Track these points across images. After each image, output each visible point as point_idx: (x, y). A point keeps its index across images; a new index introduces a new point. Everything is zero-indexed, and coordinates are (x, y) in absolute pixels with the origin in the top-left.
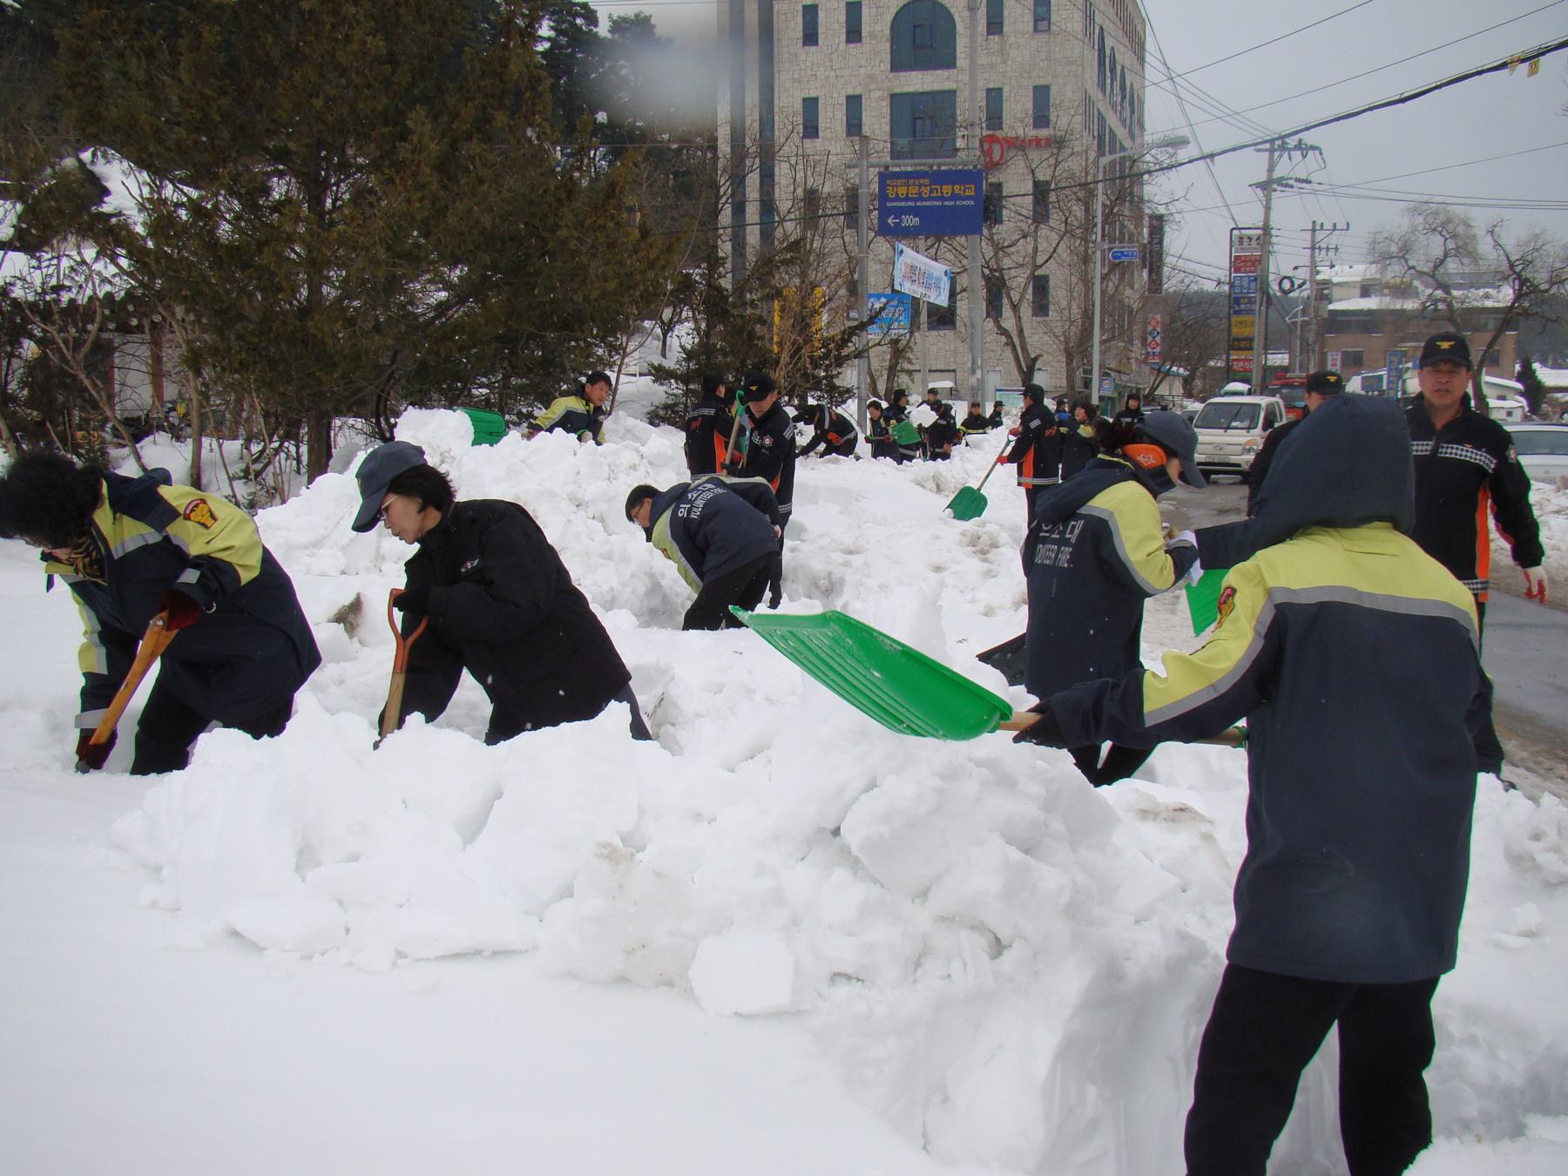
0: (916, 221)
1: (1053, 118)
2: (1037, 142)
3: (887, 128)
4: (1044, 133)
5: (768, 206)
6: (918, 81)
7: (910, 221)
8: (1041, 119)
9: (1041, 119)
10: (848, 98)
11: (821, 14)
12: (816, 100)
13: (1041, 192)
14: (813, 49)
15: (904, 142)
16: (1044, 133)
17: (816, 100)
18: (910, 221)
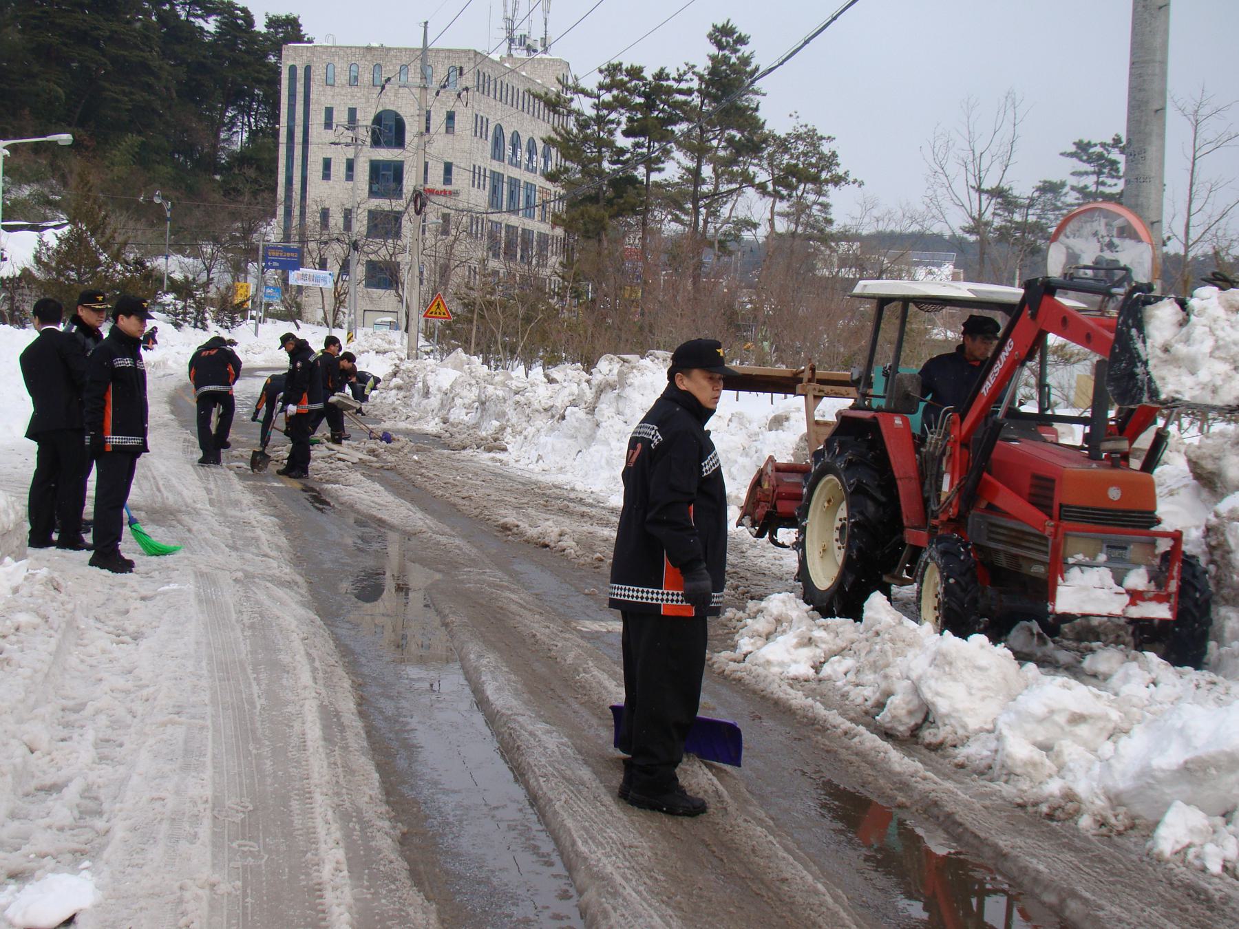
0: (277, 264)
1: (453, 181)
2: (444, 193)
3: (367, 178)
4: (448, 188)
6: (386, 154)
7: (276, 264)
8: (448, 179)
9: (448, 179)
10: (348, 160)
11: (335, 113)
12: (330, 159)
13: (446, 218)
14: (330, 131)
15: (375, 188)
17: (330, 159)
18: (276, 264)
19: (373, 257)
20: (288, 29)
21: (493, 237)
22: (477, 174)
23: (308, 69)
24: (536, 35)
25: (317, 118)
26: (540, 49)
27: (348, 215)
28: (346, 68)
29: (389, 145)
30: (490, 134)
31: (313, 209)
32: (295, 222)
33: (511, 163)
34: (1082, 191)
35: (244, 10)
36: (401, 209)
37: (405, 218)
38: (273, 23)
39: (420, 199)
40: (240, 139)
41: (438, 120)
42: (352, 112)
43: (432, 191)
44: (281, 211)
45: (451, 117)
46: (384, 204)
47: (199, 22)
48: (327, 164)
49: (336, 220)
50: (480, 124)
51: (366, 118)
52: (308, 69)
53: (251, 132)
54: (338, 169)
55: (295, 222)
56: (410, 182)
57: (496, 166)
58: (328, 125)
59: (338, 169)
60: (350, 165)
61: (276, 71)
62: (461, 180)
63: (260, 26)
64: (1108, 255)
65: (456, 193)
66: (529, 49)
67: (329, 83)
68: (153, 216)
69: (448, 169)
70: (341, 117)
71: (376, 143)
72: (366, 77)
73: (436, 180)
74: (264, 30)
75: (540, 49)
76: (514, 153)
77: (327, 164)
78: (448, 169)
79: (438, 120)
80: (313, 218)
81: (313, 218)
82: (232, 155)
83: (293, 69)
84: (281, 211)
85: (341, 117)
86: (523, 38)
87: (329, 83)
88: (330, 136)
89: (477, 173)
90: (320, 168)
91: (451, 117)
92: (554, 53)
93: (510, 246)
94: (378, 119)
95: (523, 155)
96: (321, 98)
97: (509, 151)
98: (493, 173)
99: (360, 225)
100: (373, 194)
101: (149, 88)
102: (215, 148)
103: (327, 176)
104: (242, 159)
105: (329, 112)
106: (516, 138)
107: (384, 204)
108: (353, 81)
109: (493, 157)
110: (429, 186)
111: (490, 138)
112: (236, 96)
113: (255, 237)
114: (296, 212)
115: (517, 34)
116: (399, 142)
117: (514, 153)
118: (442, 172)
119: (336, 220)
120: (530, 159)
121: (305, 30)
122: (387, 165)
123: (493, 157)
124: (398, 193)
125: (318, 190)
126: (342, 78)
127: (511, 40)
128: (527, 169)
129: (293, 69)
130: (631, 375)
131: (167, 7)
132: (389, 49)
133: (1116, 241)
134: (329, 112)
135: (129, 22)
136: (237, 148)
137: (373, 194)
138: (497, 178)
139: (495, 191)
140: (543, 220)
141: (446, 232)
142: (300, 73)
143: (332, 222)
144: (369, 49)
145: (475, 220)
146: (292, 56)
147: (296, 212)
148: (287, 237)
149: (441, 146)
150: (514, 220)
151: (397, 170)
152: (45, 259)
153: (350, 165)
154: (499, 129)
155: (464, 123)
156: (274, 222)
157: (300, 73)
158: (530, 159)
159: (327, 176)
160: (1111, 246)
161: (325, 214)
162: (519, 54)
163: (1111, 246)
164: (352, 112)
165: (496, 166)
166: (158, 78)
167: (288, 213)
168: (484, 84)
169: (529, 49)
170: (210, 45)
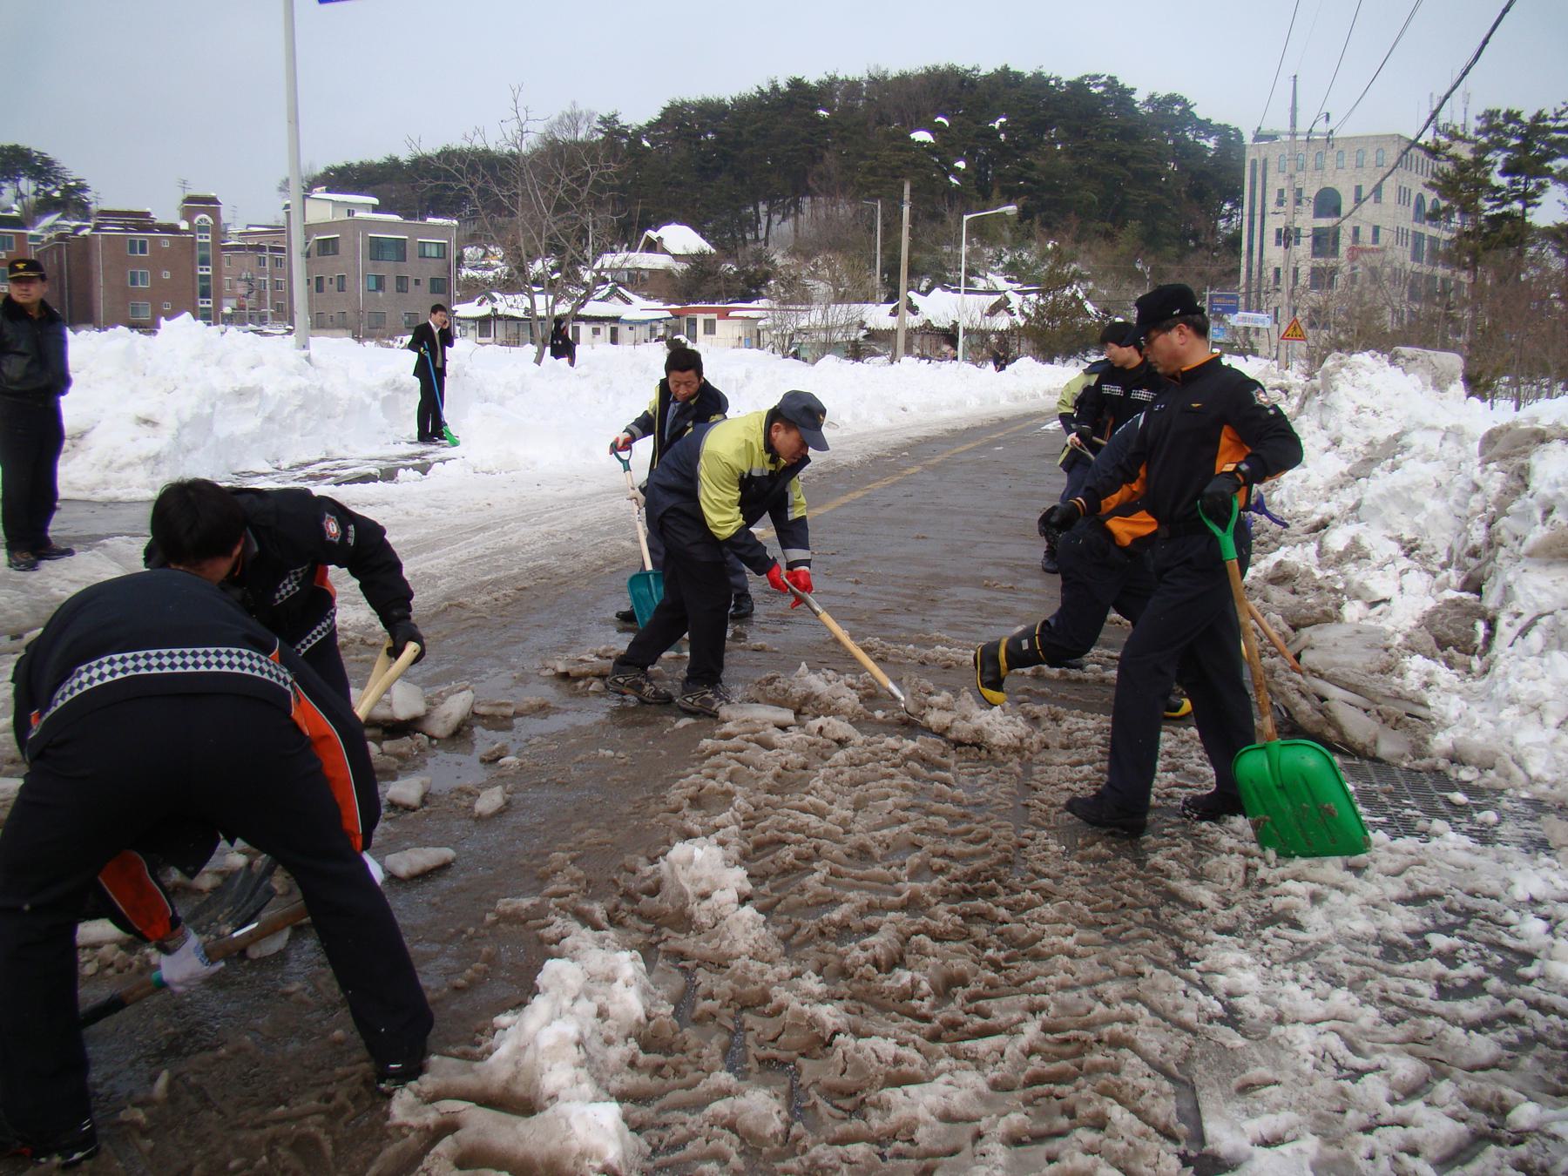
4: (1376, 246)
6: (1324, 223)
15: (1317, 248)
16: (1376, 246)
22: (1400, 233)
35: (1236, 130)
46: (1321, 262)
47: (1203, 142)
51: (1311, 192)
52: (1265, 161)
56: (1345, 242)
65: (1383, 250)
69: (1376, 230)
71: (1318, 214)
78: (1376, 230)
83: (1254, 162)
98: (1414, 232)
99: (1304, 279)
100: (1314, 254)
107: (1321, 262)
110: (1360, 245)
111: (1412, 205)
116: (1336, 211)
118: (1371, 234)
129: (1254, 162)
130: (1338, 376)
151: (1335, 233)
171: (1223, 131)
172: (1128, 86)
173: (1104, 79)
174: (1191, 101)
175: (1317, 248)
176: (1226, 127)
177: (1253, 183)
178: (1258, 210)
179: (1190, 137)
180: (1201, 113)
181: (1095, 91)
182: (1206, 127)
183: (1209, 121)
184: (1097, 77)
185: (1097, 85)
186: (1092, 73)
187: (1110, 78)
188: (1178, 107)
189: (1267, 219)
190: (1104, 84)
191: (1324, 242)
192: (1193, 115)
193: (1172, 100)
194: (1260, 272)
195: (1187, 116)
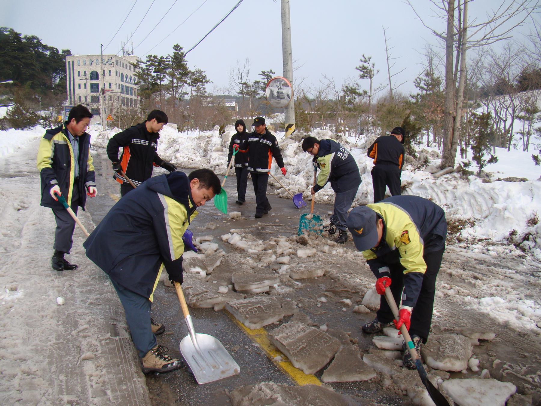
4: (111, 89)
5: (74, 98)
6: (94, 82)
8: (110, 87)
9: (110, 87)
13: (111, 96)
15: (92, 90)
19: (93, 107)
20: (68, 52)
21: (123, 101)
22: (117, 85)
23: (73, 62)
24: (130, 50)
25: (76, 74)
26: (131, 53)
27: (86, 97)
28: (83, 61)
29: (95, 79)
30: (120, 75)
31: (76, 96)
32: (73, 100)
33: (126, 82)
34: (264, 83)
35: (56, 49)
36: (98, 95)
37: (100, 97)
38: (64, 51)
39: (104, 91)
40: (57, 81)
41: (107, 73)
42: (85, 72)
43: (106, 90)
44: (69, 97)
45: (110, 71)
46: (95, 94)
47: (45, 52)
48: (80, 85)
49: (83, 99)
50: (117, 73)
51: (88, 73)
52: (73, 62)
53: (60, 79)
54: (83, 86)
55: (73, 100)
56: (100, 88)
57: (122, 83)
58: (79, 75)
59: (83, 86)
60: (85, 85)
61: (65, 63)
62: (114, 87)
63: (61, 52)
64: (280, 91)
65: (113, 90)
66: (129, 54)
67: (79, 65)
68: (36, 101)
69: (110, 84)
70: (82, 73)
71: (92, 79)
72: (88, 63)
73: (107, 87)
74: (62, 53)
75: (131, 53)
76: (127, 80)
77: (80, 85)
78: (110, 84)
79: (107, 73)
80: (77, 99)
81: (77, 99)
82: (56, 85)
83: (69, 62)
84: (69, 97)
85: (82, 73)
86: (127, 52)
87: (79, 65)
88: (80, 78)
89: (117, 85)
90: (78, 86)
91: (110, 71)
92: (135, 55)
93: (127, 102)
94: (92, 73)
95: (129, 80)
96: (77, 69)
97: (125, 79)
99: (89, 100)
100: (92, 92)
101: (33, 69)
102: (51, 83)
103: (80, 88)
104: (58, 85)
105: (79, 72)
106: (127, 76)
107: (95, 94)
108: (85, 64)
109: (121, 81)
112: (55, 70)
113: (63, 105)
114: (73, 97)
115: (125, 51)
116: (97, 78)
117: (127, 80)
119: (83, 99)
120: (131, 81)
121: (72, 53)
122: (95, 84)
123: (121, 81)
124: (98, 91)
125: (77, 91)
126: (82, 63)
127: (124, 52)
128: (130, 83)
129: (69, 62)
131: (37, 49)
132: (93, 56)
133: (282, 87)
134: (79, 72)
135: (27, 53)
136: (57, 83)
137: (92, 92)
138: (122, 86)
139: (122, 89)
140: (135, 96)
141: (111, 100)
142: (71, 63)
143: (82, 99)
144: (88, 56)
145: (118, 97)
146: (69, 59)
147: (73, 97)
148: (71, 104)
149: (107, 79)
150: (127, 96)
151: (97, 85)
152: (9, 113)
153: (85, 85)
154: (122, 74)
155: (113, 74)
156: (67, 101)
157: (71, 63)
158: (131, 81)
159: (80, 88)
160: (281, 88)
161: (80, 98)
162: (126, 55)
163: (281, 88)
164: (85, 72)
165: (122, 83)
166: (36, 67)
167: (71, 98)
168: (118, 63)
169: (129, 54)
170: (48, 58)
171: (52, 49)
172: (18, 33)
173: (9, 30)
174: (40, 38)
175: (92, 90)
176: (53, 48)
177: (69, 69)
178: (72, 78)
179: (41, 51)
180: (44, 43)
181: (6, 33)
182: (45, 47)
183: (46, 46)
184: (6, 28)
185: (6, 31)
186: (4, 26)
187: (11, 29)
188: (35, 41)
189: (75, 81)
190: (9, 31)
191: (95, 87)
192: (41, 43)
193: (33, 38)
194: (74, 98)
195: (39, 44)
